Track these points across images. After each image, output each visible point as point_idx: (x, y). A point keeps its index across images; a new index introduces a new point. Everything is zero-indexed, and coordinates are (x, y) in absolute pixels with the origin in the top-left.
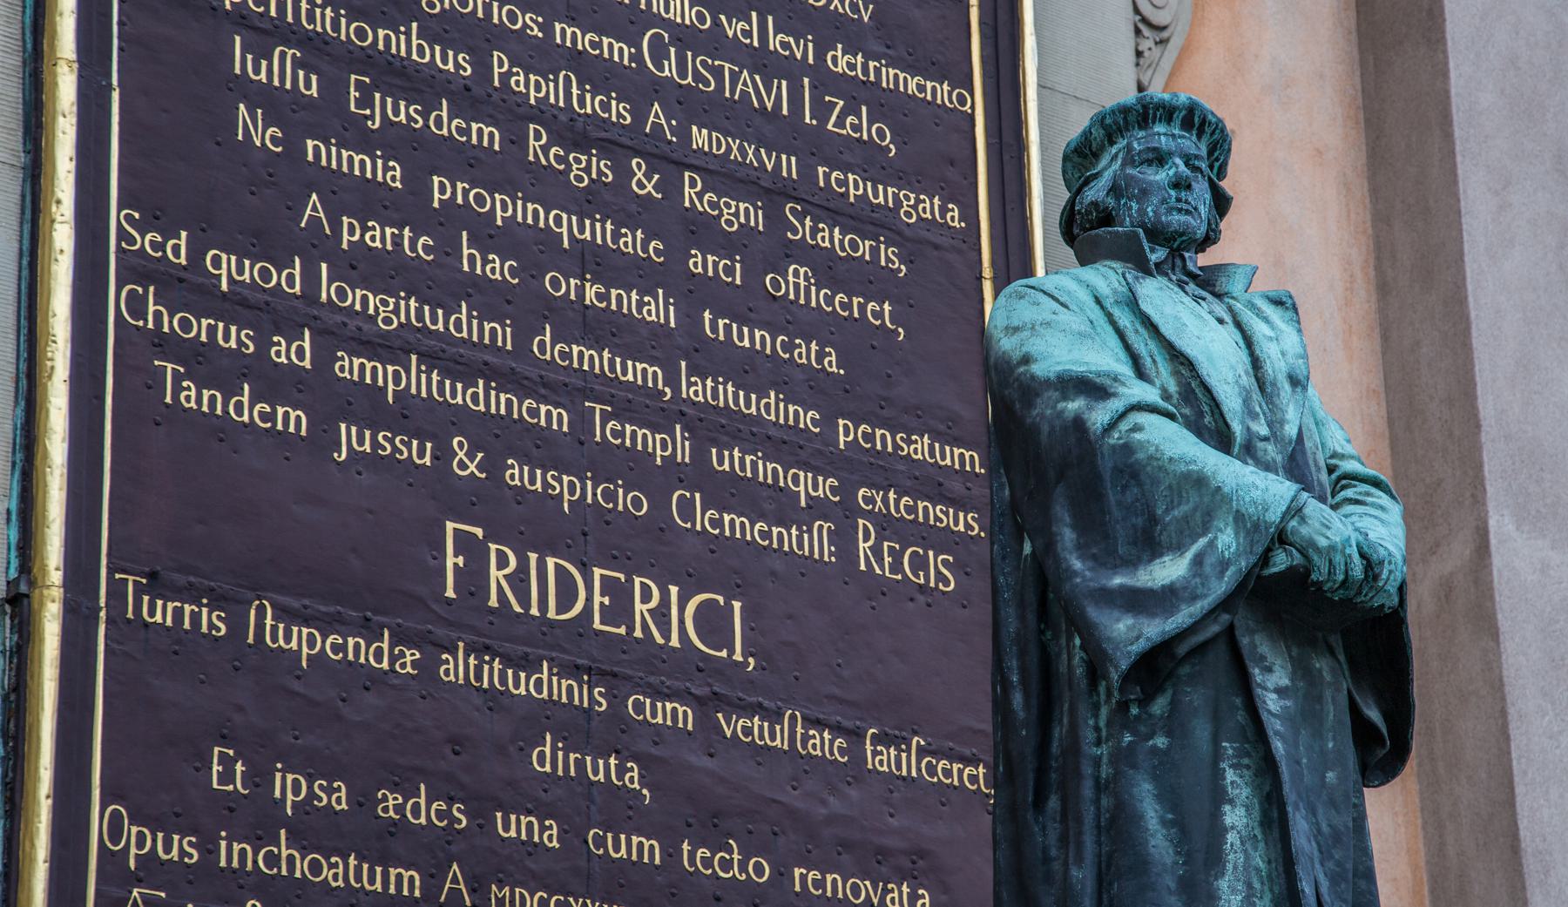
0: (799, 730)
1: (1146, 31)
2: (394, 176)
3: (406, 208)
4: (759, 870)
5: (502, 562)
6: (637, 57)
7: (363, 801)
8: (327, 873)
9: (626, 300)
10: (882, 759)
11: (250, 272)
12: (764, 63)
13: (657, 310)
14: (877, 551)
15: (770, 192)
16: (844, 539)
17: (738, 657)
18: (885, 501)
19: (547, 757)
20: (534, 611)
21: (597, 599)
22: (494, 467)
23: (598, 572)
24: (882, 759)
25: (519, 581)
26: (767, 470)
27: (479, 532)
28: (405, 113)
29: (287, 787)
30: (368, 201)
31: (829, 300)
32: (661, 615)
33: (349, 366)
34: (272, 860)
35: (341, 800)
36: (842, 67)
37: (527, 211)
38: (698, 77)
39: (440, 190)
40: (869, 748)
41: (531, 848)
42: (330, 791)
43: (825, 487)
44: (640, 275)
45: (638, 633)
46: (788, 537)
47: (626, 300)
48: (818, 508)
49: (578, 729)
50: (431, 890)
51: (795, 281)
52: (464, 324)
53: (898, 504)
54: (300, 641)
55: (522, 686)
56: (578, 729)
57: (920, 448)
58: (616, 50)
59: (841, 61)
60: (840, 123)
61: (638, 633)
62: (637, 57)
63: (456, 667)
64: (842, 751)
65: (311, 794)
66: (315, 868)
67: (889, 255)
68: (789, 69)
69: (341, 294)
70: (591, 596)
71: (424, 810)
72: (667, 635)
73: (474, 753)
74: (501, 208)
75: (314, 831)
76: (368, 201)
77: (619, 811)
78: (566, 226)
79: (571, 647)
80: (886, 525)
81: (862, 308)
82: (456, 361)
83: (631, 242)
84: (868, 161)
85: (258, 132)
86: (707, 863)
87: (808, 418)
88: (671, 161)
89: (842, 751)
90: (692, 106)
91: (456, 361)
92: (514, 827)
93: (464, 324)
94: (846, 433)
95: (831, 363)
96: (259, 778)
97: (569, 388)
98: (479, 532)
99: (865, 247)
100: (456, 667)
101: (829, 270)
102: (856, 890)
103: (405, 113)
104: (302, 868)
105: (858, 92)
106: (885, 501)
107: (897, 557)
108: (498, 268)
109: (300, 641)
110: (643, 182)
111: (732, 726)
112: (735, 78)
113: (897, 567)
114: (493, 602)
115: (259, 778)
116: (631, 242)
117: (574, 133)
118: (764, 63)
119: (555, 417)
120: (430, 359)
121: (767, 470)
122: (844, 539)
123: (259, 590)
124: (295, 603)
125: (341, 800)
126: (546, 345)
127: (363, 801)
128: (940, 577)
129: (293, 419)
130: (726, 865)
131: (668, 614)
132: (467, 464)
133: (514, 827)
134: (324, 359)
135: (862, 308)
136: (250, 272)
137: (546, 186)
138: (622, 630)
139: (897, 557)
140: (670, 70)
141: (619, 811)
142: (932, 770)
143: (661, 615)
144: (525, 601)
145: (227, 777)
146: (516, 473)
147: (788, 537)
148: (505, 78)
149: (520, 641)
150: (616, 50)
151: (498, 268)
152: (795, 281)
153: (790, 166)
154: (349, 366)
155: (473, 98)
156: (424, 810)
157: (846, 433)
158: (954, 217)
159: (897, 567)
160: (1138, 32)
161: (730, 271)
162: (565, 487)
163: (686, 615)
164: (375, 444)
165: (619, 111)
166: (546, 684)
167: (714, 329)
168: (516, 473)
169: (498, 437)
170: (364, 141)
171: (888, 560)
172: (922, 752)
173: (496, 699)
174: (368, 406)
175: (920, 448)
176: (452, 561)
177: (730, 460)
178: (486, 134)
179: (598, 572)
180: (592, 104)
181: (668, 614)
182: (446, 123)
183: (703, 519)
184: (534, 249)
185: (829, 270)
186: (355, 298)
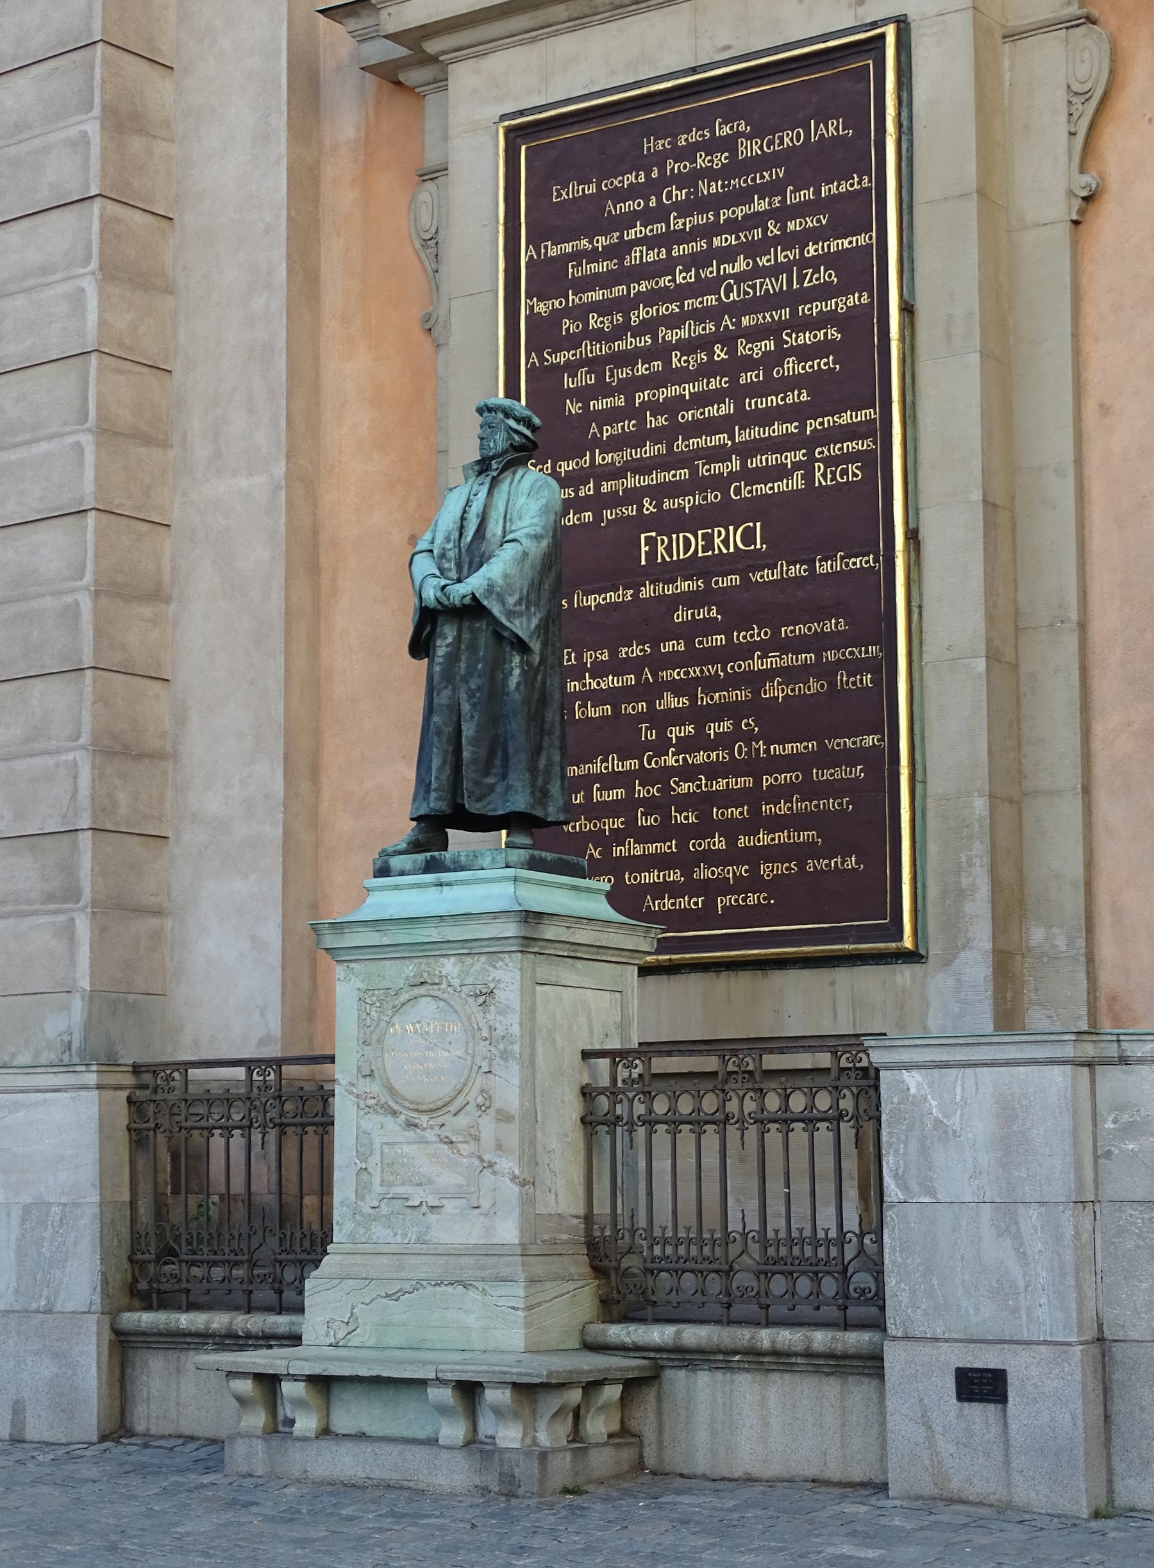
0: (785, 568)
1: (1074, 100)
2: (621, 401)
3: (630, 412)
4: (766, 634)
5: (663, 541)
6: (719, 299)
7: (614, 654)
8: (602, 685)
9: (712, 411)
10: (824, 568)
11: (572, 465)
12: (775, 271)
13: (726, 408)
14: (824, 475)
15: (772, 331)
16: (809, 477)
17: (758, 546)
18: (829, 450)
19: (682, 615)
20: (675, 558)
21: (701, 543)
22: (659, 506)
23: (700, 532)
24: (824, 568)
25: (669, 549)
26: (772, 459)
27: (654, 534)
28: (624, 373)
29: (588, 658)
30: (612, 416)
31: (804, 368)
32: (726, 542)
33: (606, 487)
34: (584, 685)
35: (605, 657)
36: (812, 253)
37: (673, 391)
38: (747, 293)
39: (641, 397)
40: (818, 565)
41: (675, 653)
42: (601, 654)
43: (800, 455)
44: (717, 397)
45: (717, 552)
46: (782, 486)
47: (712, 411)
48: (797, 466)
49: (692, 600)
50: (638, 680)
51: (791, 366)
52: (650, 450)
53: (835, 450)
54: (592, 601)
55: (669, 590)
56: (692, 600)
57: (846, 418)
58: (710, 300)
59: (811, 250)
60: (811, 281)
61: (717, 552)
62: (719, 299)
63: (647, 591)
64: (805, 571)
65: (597, 657)
66: (598, 684)
67: (833, 334)
68: (786, 268)
69: (603, 459)
70: (697, 543)
71: (636, 651)
72: (728, 548)
73: (651, 622)
74: (663, 394)
75: (599, 671)
76: (612, 416)
77: (709, 627)
78: (688, 390)
79: (691, 567)
80: (829, 462)
81: (819, 364)
82: (642, 467)
83: (714, 384)
84: (824, 292)
85: (573, 407)
86: (745, 637)
87: (792, 428)
88: (728, 340)
89: (805, 571)
90: (737, 310)
91: (642, 467)
92: (669, 646)
93: (650, 450)
94: (812, 425)
95: (804, 397)
96: (579, 657)
97: (687, 460)
98: (654, 534)
99: (821, 335)
100: (647, 591)
101: (804, 353)
102: (810, 629)
103: (624, 373)
104: (594, 685)
105: (814, 263)
106: (829, 450)
107: (833, 473)
108: (662, 421)
109: (592, 601)
110: (720, 354)
111: (757, 577)
112: (762, 284)
113: (834, 478)
114: (659, 560)
115: (579, 657)
116: (714, 384)
117: (688, 347)
118: (775, 271)
119: (684, 474)
120: (635, 472)
121: (772, 459)
122: (809, 477)
123: (577, 587)
124: (588, 587)
125: (605, 657)
126: (680, 445)
127: (614, 654)
128: (855, 475)
129: (588, 516)
130: (752, 636)
131: (730, 539)
132: (648, 507)
133: (669, 646)
134: (597, 487)
135: (819, 364)
136: (572, 465)
137: (684, 376)
138: (710, 553)
139: (833, 473)
140: (733, 296)
141: (709, 627)
142: (847, 565)
143: (726, 542)
144: (671, 556)
145: (569, 660)
146: (667, 504)
147: (782, 486)
148: (663, 337)
149: (667, 572)
150: (710, 300)
151: (662, 421)
152: (791, 366)
153: (786, 313)
154: (606, 487)
155: (647, 355)
156: (636, 651)
157: (812, 425)
158: (865, 300)
159: (834, 478)
160: (1070, 102)
161: (757, 376)
162: (687, 503)
163: (736, 538)
164: (617, 514)
165: (711, 327)
166: (685, 586)
167: (750, 405)
168: (667, 504)
169: (659, 492)
170: (609, 392)
171: (829, 476)
172: (842, 558)
173: (661, 598)
174: (614, 500)
175: (846, 418)
176: (644, 549)
177: (754, 463)
178: (658, 365)
179: (700, 532)
180: (699, 330)
181: (730, 539)
182: (642, 369)
183: (745, 493)
184: (675, 405)
185: (804, 353)
186: (608, 458)
